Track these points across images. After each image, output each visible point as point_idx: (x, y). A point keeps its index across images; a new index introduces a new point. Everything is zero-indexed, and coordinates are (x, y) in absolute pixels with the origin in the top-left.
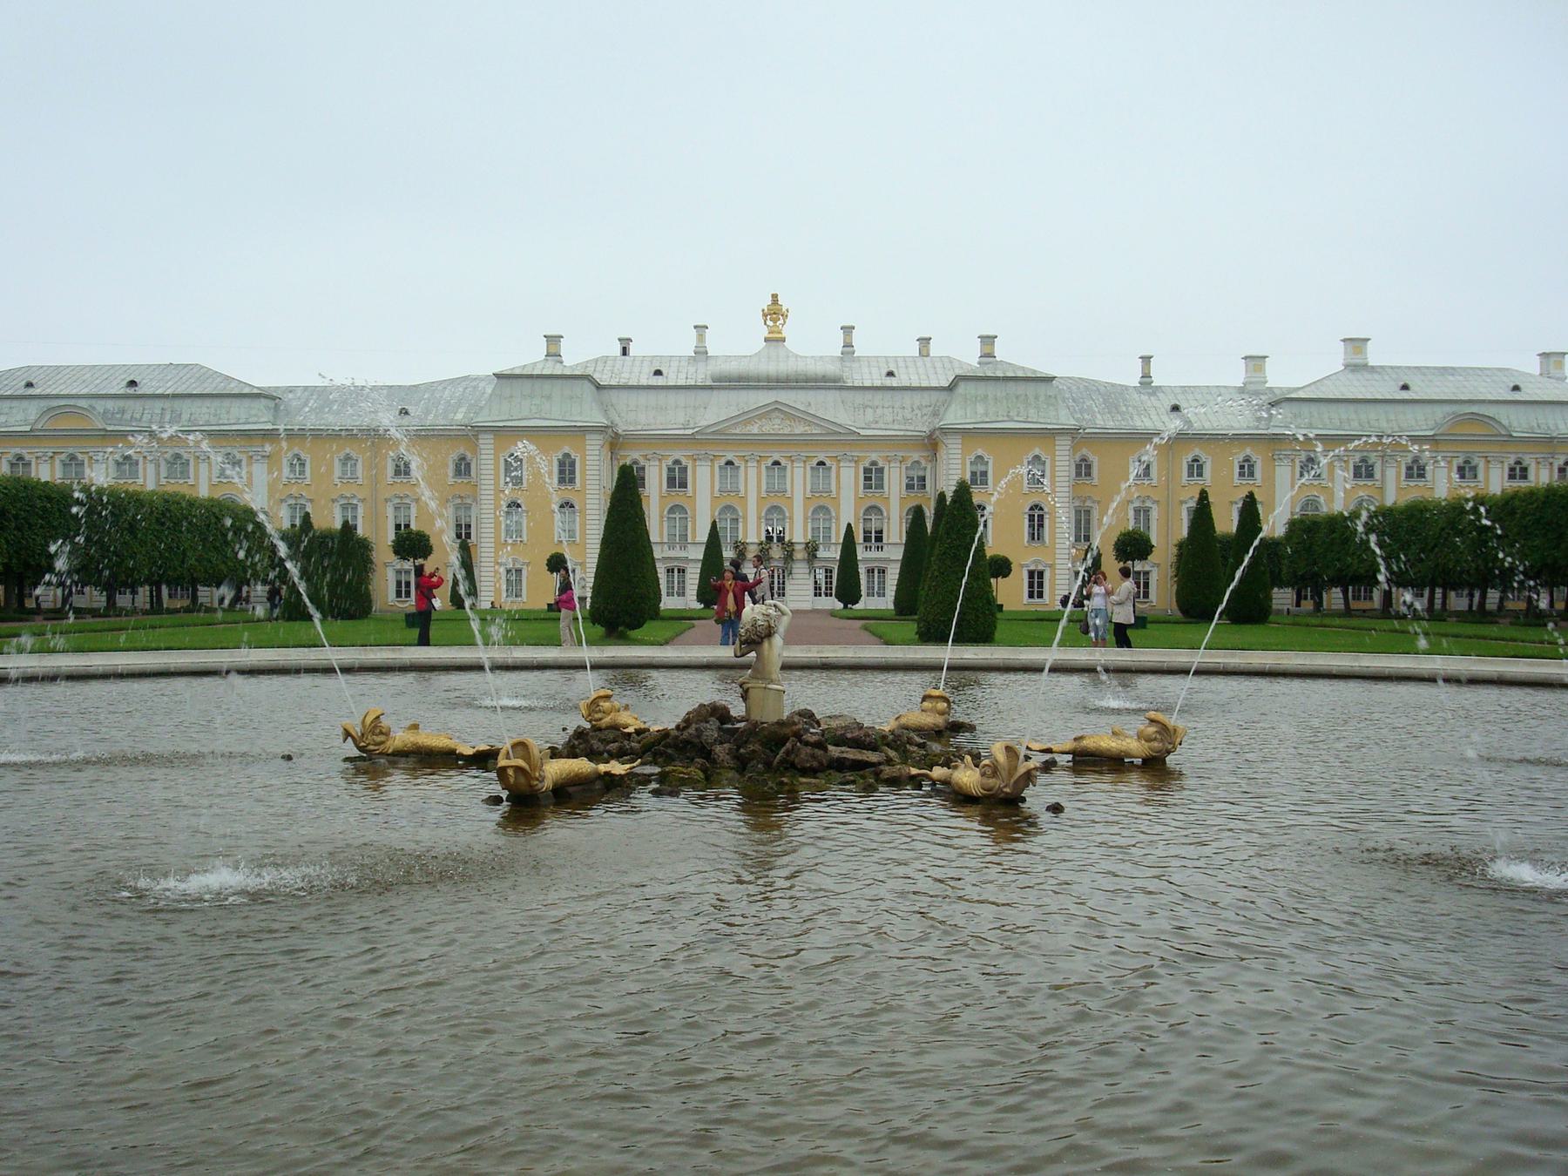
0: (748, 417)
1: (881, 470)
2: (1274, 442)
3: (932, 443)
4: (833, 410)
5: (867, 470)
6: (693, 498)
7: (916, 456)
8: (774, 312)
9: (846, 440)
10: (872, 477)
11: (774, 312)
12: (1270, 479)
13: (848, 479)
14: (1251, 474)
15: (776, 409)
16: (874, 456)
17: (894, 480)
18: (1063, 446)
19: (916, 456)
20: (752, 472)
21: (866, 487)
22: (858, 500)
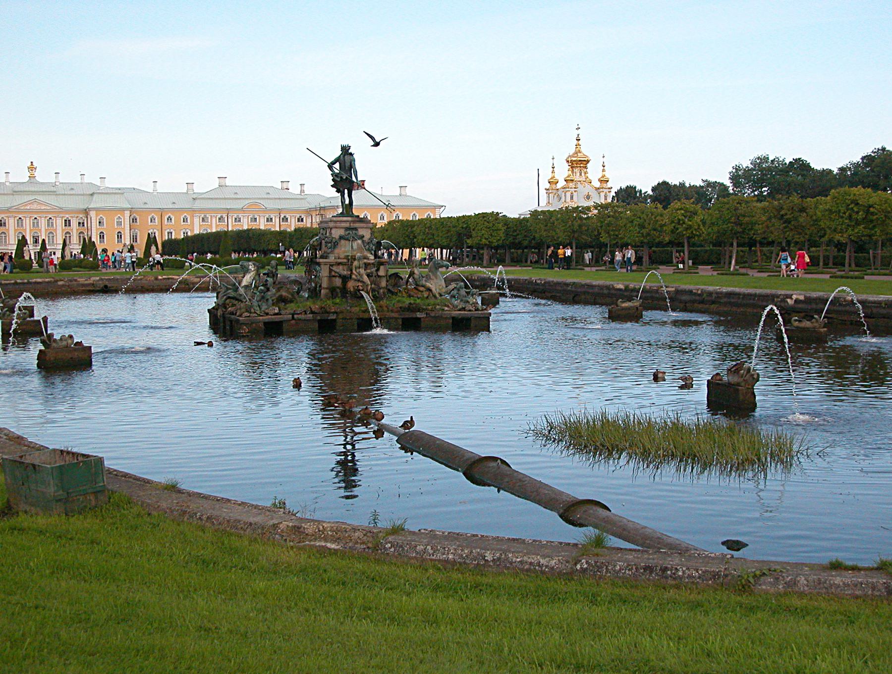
0: (26, 204)
1: (69, 221)
2: (193, 211)
3: (86, 212)
4: (53, 201)
5: (65, 221)
6: (8, 230)
7: (81, 216)
8: (32, 168)
9: (61, 211)
10: (67, 223)
11: (32, 168)
12: (192, 223)
13: (59, 223)
14: (187, 221)
15: (35, 201)
16: (67, 216)
17: (74, 223)
18: (127, 213)
19: (81, 216)
20: (28, 221)
21: (65, 226)
22: (63, 230)
